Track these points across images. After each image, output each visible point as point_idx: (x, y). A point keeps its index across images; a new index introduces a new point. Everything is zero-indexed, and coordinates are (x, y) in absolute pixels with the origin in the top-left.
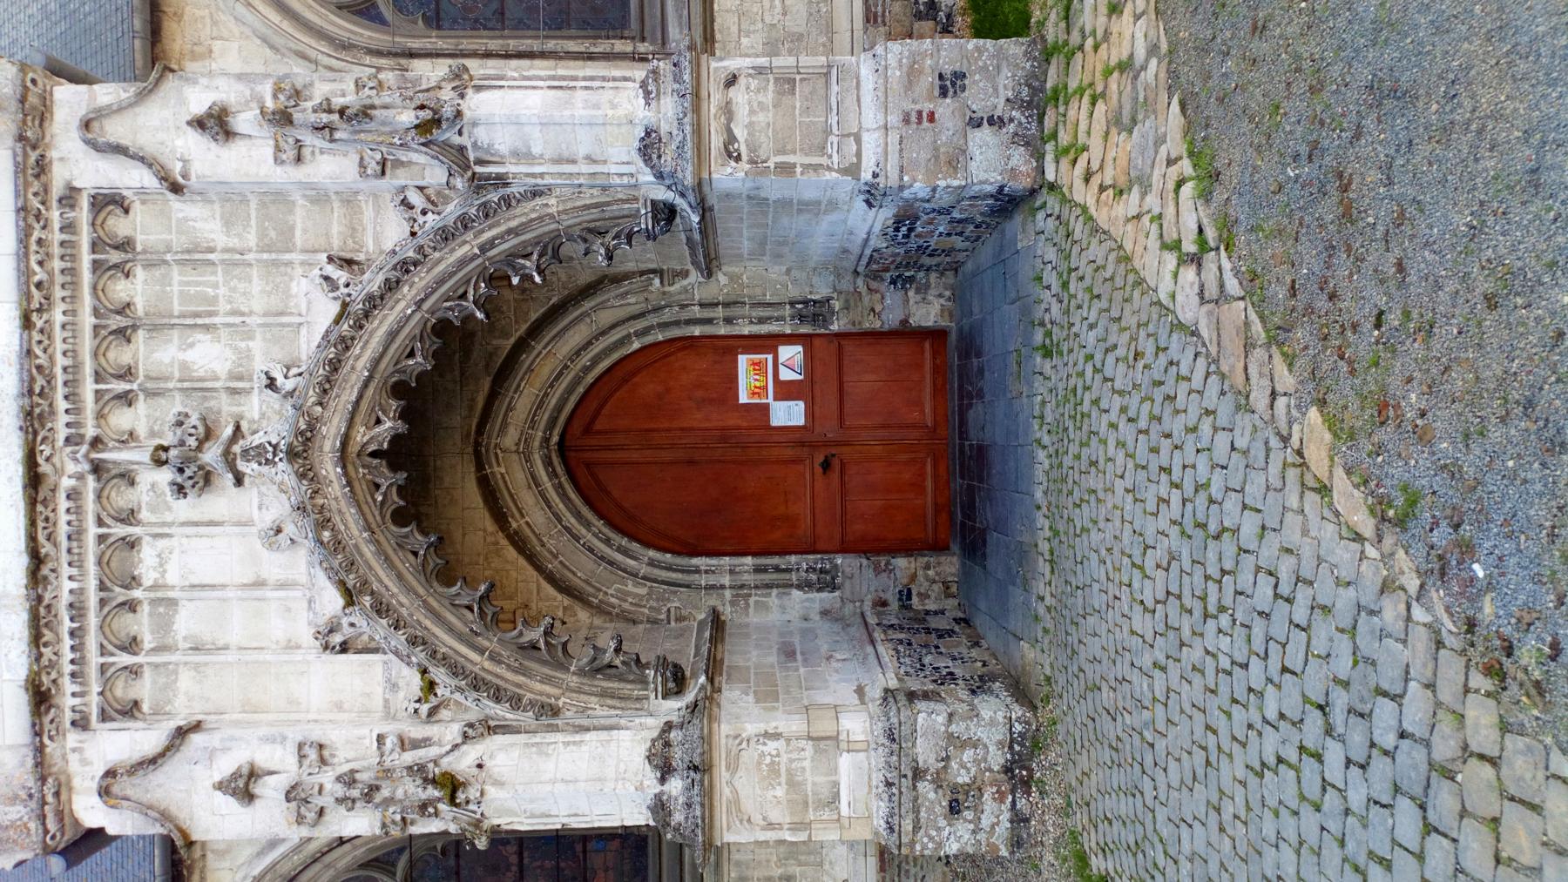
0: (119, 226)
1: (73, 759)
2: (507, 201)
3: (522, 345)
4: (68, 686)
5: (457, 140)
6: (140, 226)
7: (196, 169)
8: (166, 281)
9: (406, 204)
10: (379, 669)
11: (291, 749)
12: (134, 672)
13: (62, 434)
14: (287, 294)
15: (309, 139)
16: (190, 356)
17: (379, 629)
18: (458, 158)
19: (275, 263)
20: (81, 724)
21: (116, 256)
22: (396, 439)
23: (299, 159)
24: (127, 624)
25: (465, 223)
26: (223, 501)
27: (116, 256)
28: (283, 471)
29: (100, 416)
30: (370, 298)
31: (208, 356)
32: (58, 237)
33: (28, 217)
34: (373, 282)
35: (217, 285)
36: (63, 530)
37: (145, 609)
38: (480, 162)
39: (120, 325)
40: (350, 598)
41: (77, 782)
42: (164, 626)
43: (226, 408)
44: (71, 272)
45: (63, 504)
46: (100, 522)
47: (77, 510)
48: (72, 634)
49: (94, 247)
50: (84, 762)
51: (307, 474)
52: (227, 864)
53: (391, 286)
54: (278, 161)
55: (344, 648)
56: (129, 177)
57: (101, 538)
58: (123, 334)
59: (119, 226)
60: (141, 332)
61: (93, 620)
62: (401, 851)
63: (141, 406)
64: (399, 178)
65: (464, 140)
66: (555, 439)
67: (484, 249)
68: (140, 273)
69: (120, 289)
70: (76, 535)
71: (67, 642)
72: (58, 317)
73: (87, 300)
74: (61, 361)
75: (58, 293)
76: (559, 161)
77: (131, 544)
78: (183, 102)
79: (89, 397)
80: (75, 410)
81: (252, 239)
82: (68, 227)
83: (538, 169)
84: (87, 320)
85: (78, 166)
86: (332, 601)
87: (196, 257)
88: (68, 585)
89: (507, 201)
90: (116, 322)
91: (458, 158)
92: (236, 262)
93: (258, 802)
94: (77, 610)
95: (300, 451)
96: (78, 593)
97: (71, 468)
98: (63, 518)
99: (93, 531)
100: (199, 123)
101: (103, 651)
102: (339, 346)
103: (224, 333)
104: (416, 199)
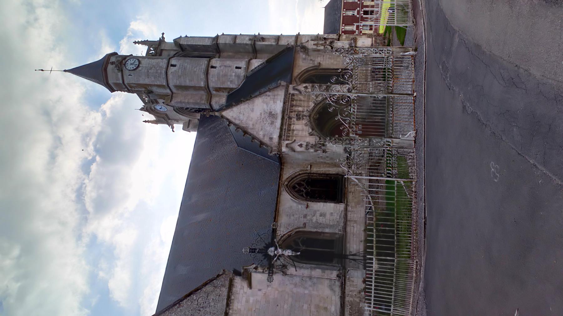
6: (295, 97)
12: (289, 136)
17: (315, 133)
26: (300, 122)
27: (292, 100)
28: (308, 118)
31: (300, 109)
33: (286, 95)
35: (302, 103)
39: (292, 106)
40: (313, 130)
42: (293, 133)
55: (312, 135)
58: (292, 106)
77: (290, 125)
85: (291, 91)
86: (311, 131)
87: (300, 100)
94: (285, 129)
95: (310, 116)
100: (304, 87)
102: (314, 107)
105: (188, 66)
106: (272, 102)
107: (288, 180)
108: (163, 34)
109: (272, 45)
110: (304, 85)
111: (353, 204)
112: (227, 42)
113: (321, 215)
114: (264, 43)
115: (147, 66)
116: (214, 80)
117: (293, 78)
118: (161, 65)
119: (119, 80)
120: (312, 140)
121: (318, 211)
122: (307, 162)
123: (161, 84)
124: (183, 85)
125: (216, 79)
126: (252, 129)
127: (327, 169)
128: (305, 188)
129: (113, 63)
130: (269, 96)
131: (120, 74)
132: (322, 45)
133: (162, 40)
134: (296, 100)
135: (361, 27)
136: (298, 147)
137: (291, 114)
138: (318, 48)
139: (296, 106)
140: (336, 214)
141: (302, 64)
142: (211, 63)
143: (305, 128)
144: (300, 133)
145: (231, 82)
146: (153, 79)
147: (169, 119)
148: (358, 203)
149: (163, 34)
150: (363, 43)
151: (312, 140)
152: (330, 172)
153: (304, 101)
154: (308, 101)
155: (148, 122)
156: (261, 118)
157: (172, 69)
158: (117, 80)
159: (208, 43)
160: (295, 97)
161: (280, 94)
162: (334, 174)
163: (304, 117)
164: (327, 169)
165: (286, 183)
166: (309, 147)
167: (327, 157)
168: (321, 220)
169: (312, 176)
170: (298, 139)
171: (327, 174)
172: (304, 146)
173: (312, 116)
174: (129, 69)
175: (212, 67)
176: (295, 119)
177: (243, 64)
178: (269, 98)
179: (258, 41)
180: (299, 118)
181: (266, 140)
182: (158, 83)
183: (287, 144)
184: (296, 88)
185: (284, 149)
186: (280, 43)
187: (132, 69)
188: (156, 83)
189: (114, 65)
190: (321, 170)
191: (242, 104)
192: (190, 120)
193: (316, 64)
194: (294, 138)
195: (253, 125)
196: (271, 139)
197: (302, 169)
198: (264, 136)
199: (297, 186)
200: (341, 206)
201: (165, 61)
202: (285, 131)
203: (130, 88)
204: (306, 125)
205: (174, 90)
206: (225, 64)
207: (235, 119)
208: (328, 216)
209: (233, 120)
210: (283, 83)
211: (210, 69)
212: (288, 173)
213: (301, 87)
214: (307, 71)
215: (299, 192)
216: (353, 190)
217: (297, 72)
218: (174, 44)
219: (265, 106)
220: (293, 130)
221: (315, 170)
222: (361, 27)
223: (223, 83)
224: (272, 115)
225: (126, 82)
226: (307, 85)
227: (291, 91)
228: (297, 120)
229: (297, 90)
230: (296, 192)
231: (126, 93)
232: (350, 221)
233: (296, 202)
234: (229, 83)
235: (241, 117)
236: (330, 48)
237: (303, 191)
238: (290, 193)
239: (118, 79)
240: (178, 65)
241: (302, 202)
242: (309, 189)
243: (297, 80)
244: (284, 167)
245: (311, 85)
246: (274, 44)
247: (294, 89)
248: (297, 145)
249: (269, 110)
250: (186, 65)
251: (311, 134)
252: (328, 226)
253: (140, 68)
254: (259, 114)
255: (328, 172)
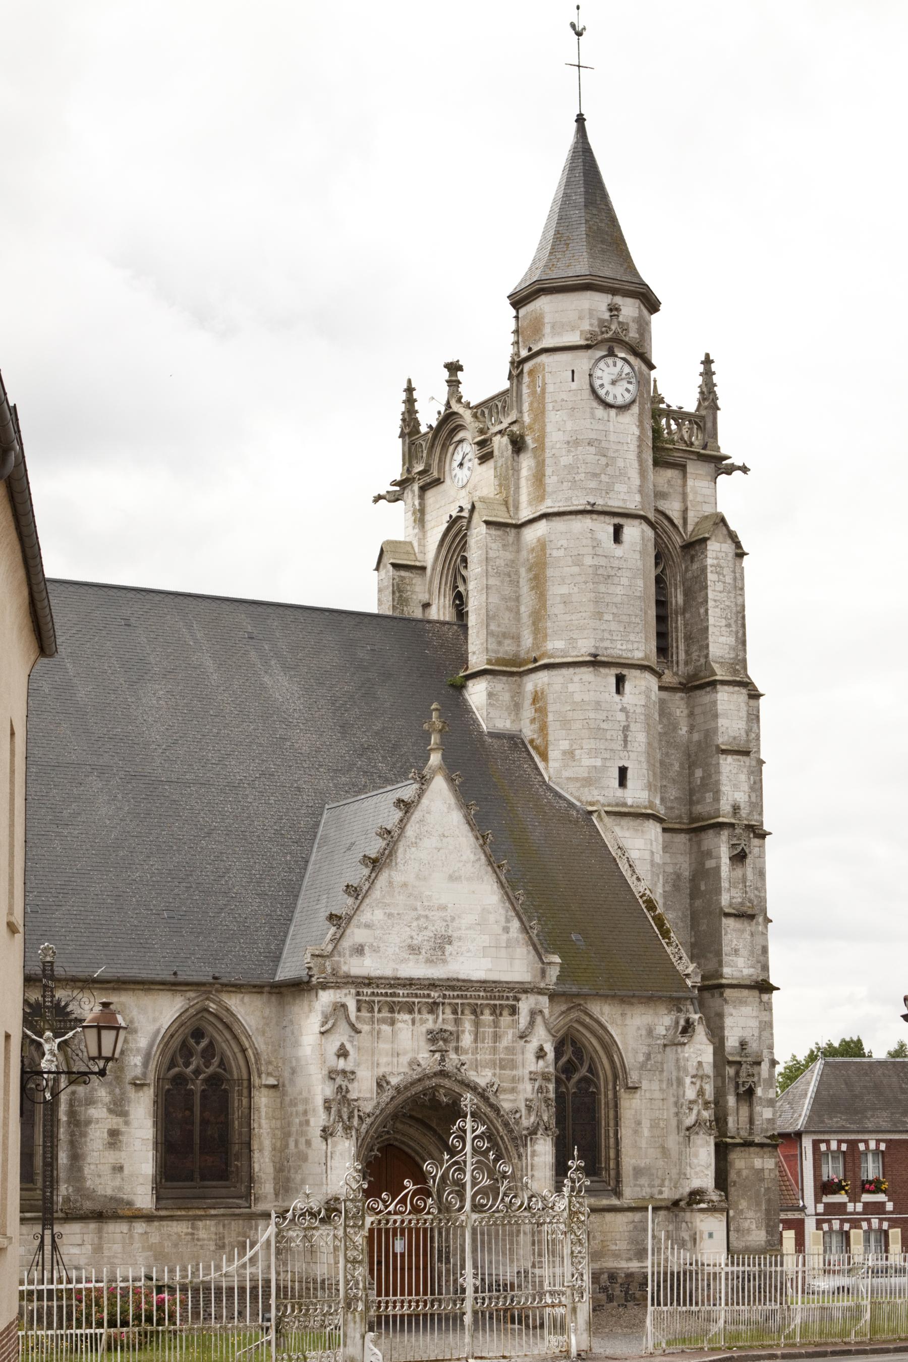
0: (506, 1012)
1: (347, 991)
2: (517, 1146)
3: (435, 1131)
4: (370, 991)
5: (539, 1133)
6: (506, 1019)
7: (528, 1045)
8: (490, 1027)
9: (517, 1112)
10: (369, 1095)
11: (353, 1069)
12: (371, 1010)
13: (447, 993)
14: (485, 1067)
15: (537, 1085)
16: (467, 1033)
17: (386, 1097)
18: (533, 1132)
19: (495, 1064)
20: (358, 994)
21: (496, 1011)
22: (439, 1102)
23: (531, 1079)
24: (385, 1009)
25: (511, 1131)
27: (496, 1011)
29: (450, 1004)
30: (488, 1098)
31: (467, 1040)
32: (505, 995)
34: (493, 1100)
35: (488, 1043)
36: (419, 992)
37: (390, 1015)
38: (531, 1139)
39: (476, 1011)
40: (398, 1089)
41: (338, 991)
42: (383, 1021)
43: (453, 1044)
44: (495, 998)
45: (426, 992)
46: (419, 1003)
47: (424, 996)
48: (386, 993)
49: (500, 1005)
50: (346, 995)
51: (435, 1074)
52: (238, 1002)
53: (492, 1106)
54: (531, 1073)
55: (379, 1085)
56: (523, 1019)
57: (414, 1003)
58: (474, 1012)
59: (506, 1012)
60: (473, 1017)
61: (389, 999)
62: (225, 1070)
63: (452, 1016)
64: (524, 1111)
65: (539, 1136)
66: (396, 1143)
67: (501, 1137)
68: (492, 1018)
69: (487, 1012)
70: (416, 996)
71: (383, 991)
72: (482, 994)
73: (486, 1002)
74: (468, 994)
75: (488, 994)
76: (532, 1166)
77: (411, 1012)
78: (546, 1042)
79: (456, 1001)
80: (454, 998)
81: (502, 1056)
82: (508, 998)
83: (529, 1158)
84: (479, 1002)
86: (394, 1081)
87: (496, 1037)
88: (401, 992)
89: (517, 1146)
90: (478, 1010)
91: (533, 1132)
92: (494, 1050)
93: (336, 1058)
95: (443, 1074)
96: (399, 996)
97: (436, 995)
98: (422, 992)
99: (416, 1000)
100: (541, 1049)
101: (379, 1002)
103: (474, 1045)
104: (518, 1116)
105: (619, 590)
106: (485, 940)
107: (223, 1014)
108: (744, 469)
109: (718, 891)
110: (549, 1048)
111: (154, 1239)
112: (721, 722)
113: (114, 1134)
114: (725, 861)
115: (612, 437)
116: (571, 688)
117: (577, 1001)
118: (617, 487)
119: (554, 334)
120: (364, 1090)
121: (127, 1123)
122: (286, 1074)
123: (549, 489)
124: (550, 572)
125: (577, 698)
126: (390, 883)
127: (267, 1143)
128: (197, 1072)
129: (614, 309)
130: (506, 930)
131: (575, 339)
132: (701, 1092)
133: (719, 465)
134: (496, 1024)
135: (875, 1223)
136: (337, 1044)
137: (448, 1010)
138: (688, 1080)
139: (477, 1024)
140: (117, 1183)
141: (632, 1030)
142: (637, 673)
143: (405, 1060)
144: (384, 1046)
145: (570, 754)
146: (565, 460)
147: (423, 489)
148: (159, 1256)
149: (744, 469)
150: (711, 1235)
151: (364, 1090)
152: (256, 1155)
153: (494, 1050)
154: (493, 1064)
155: (410, 401)
156: (430, 908)
157: (605, 529)
158: (553, 327)
159: (719, 644)
160: (506, 1019)
161: (515, 964)
162: (250, 1166)
163: (438, 1056)
164: (267, 1143)
165: (213, 1007)
166: (339, 1080)
167: (308, 1143)
168: (96, 1136)
169: (240, 1094)
170: (364, 1039)
171: (249, 1144)
172: (342, 1060)
173: (446, 1082)
174: (598, 373)
175: (620, 680)
176: (430, 1025)
177: (636, 794)
178: (498, 929)
179: (731, 837)
180: (434, 1037)
181: (356, 935)
182: (551, 481)
183: (344, 1006)
184: (539, 1019)
185: (326, 998)
186: (725, 921)
187: (597, 383)
188: (548, 471)
189: (606, 315)
190: (264, 1122)
191: (472, 839)
192: (423, 568)
193: (634, 1077)
194: (365, 1028)
195: (405, 885)
196: (359, 950)
197: (264, 1057)
198: (368, 926)
199: (204, 1043)
200: (144, 1199)
201: (633, 503)
202: (389, 997)
203: (527, 367)
204: (414, 1063)
205: (531, 534)
206: (633, 727)
207: (421, 821)
208: (111, 1157)
209: (417, 815)
210: (553, 973)
211: (614, 671)
212: (247, 1011)
213: (542, 1037)
214: (609, 1045)
215: (185, 1051)
216: (202, 1234)
217: (605, 1012)
218: (708, 510)
219: (469, 919)
220: (392, 1023)
221: (263, 1100)
222: (875, 1223)
223: (565, 723)
224: (442, 944)
225: (543, 358)
226: (551, 1056)
227: (525, 1005)
228: (430, 1032)
229: (532, 1023)
230: (184, 1044)
231: (510, 350)
232: (100, 1231)
233: (151, 1046)
234: (565, 745)
235: (429, 843)
236: (690, 1120)
237: (187, 1064)
238: (180, 1022)
239: (558, 328)
240: (618, 551)
241: (152, 1065)
242: (197, 1086)
243: (574, 1015)
244: (265, 997)
245: (551, 1069)
246: (725, 900)
247: (533, 1014)
248: (344, 1039)
249: (455, 935)
250: (624, 581)
251: (381, 1083)
252: (76, 1157)
253: (600, 412)
254: (443, 901)
255: (255, 1146)
